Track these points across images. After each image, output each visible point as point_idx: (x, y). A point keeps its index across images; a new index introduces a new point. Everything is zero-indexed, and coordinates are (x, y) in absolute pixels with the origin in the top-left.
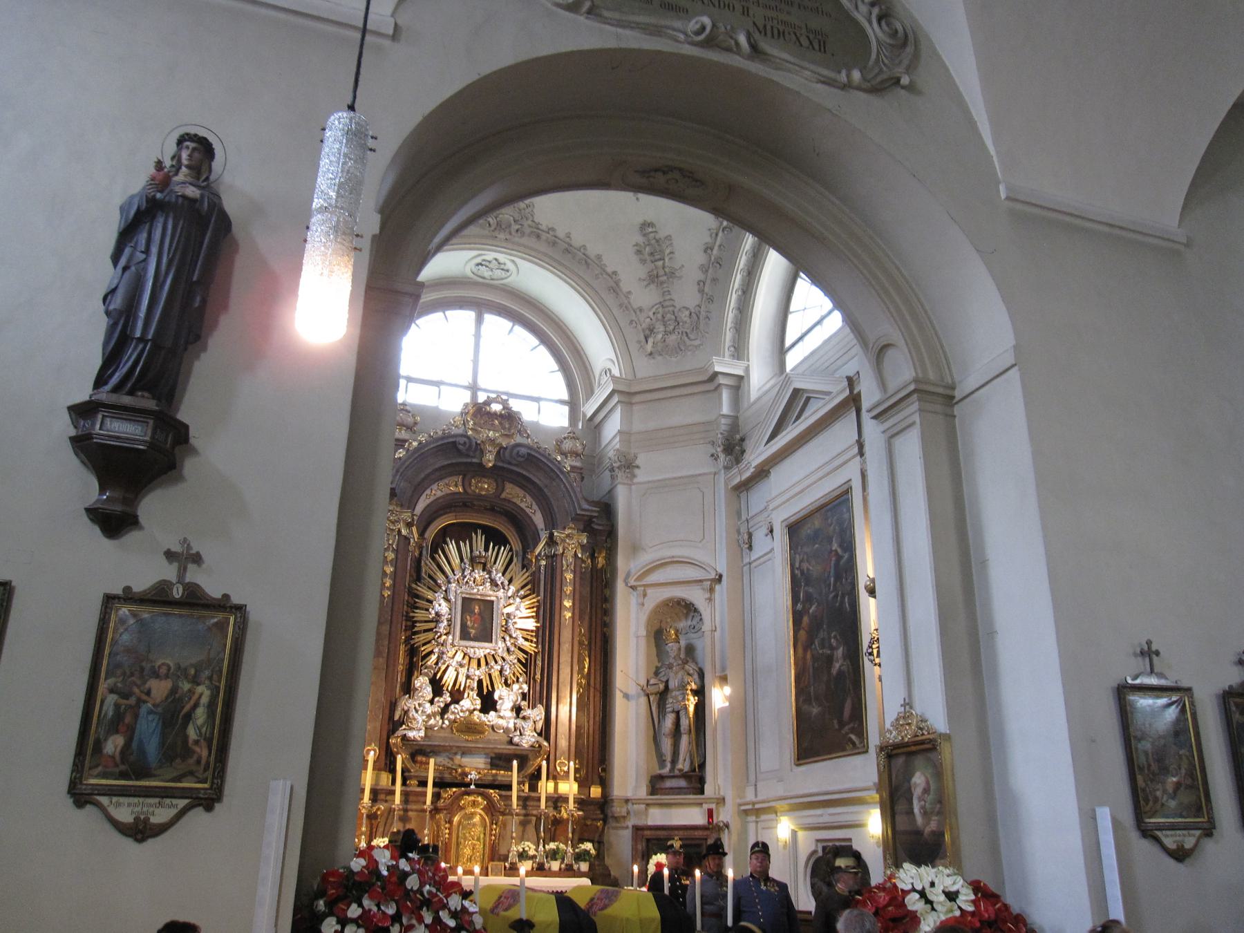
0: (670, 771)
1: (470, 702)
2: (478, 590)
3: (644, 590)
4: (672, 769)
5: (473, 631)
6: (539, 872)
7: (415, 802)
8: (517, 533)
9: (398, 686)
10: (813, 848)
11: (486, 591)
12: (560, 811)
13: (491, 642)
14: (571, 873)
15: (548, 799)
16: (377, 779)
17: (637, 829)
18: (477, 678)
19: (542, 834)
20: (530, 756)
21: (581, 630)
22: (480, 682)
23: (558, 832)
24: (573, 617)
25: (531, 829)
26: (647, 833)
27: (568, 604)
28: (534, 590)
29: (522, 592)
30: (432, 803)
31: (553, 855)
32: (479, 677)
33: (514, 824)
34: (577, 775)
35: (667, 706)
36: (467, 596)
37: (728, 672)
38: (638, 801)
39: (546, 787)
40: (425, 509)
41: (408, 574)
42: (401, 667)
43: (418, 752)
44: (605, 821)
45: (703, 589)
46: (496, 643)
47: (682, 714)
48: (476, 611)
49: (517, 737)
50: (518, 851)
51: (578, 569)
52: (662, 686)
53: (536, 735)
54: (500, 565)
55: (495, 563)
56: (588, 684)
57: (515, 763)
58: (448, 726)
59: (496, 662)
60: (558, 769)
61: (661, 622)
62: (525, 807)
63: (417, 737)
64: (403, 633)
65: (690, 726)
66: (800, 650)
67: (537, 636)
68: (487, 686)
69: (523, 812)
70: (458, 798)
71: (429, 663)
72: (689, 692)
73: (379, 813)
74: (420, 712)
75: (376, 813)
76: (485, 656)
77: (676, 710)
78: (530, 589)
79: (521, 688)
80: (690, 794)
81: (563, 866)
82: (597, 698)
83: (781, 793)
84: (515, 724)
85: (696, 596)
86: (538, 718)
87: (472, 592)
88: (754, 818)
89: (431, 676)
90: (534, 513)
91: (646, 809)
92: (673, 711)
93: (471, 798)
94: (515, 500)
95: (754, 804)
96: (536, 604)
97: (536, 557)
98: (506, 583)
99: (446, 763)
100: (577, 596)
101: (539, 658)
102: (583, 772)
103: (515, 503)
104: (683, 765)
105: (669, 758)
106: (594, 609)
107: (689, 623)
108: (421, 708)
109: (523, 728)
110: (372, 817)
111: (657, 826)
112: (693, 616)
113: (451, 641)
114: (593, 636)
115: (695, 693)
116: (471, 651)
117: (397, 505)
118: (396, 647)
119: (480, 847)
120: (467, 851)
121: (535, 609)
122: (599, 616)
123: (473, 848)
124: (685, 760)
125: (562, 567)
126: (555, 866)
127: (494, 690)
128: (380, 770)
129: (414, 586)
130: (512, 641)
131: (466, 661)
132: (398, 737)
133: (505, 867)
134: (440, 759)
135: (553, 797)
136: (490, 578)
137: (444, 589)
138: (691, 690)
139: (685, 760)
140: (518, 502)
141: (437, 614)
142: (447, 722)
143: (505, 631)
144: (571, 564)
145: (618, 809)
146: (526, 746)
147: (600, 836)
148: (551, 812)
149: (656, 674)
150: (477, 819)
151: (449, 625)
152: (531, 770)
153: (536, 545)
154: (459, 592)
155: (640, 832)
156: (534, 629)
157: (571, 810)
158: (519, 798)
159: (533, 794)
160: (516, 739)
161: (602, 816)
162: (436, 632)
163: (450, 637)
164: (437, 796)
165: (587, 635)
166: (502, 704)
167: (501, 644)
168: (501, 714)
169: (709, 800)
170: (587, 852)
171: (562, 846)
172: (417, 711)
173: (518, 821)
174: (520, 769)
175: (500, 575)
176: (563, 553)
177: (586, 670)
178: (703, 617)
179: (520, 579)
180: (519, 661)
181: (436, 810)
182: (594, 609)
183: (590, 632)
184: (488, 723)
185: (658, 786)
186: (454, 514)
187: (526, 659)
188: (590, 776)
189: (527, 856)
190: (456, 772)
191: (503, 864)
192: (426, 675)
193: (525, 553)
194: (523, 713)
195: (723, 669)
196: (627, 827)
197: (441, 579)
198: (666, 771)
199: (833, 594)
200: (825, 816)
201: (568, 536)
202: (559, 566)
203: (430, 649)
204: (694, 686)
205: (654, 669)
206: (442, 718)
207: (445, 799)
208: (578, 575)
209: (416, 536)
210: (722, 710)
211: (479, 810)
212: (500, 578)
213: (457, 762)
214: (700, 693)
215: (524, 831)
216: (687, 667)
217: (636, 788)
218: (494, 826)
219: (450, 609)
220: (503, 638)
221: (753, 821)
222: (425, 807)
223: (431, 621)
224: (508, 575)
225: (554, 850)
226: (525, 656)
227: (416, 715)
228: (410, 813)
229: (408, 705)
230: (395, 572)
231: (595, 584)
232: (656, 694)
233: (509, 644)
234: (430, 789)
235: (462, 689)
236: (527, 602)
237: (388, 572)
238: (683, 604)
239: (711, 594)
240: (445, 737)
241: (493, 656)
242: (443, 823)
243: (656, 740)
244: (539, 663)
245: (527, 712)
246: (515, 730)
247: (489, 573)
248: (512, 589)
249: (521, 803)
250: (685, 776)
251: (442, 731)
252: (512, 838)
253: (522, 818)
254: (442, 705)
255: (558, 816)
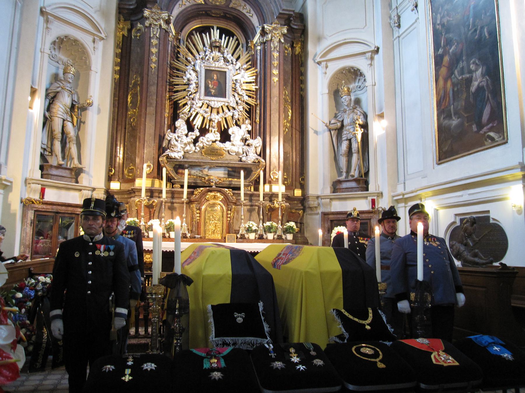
0: (345, 178)
1: (213, 136)
2: (215, 65)
3: (326, 64)
4: (347, 177)
5: (213, 91)
6: (260, 240)
7: (178, 198)
8: (243, 33)
9: (166, 126)
10: (453, 220)
11: (220, 65)
12: (274, 203)
13: (226, 97)
14: (281, 240)
15: (265, 195)
16: (153, 184)
17: (324, 214)
18: (216, 121)
19: (262, 217)
20: (253, 168)
21: (285, 93)
22: (219, 123)
23: (273, 216)
24: (279, 81)
25: (255, 214)
26: (331, 217)
27: (275, 72)
28: (254, 65)
29: (245, 66)
30: (187, 198)
31: (269, 229)
32: (218, 119)
33: (243, 210)
34: (286, 182)
35: (343, 136)
36: (208, 68)
37: (384, 111)
38: (325, 197)
39: (264, 189)
40: (179, 14)
41: (169, 56)
42: (166, 115)
43: (179, 166)
44: (304, 210)
45: (367, 58)
46: (229, 98)
47: (353, 141)
48: (215, 78)
49: (244, 157)
50: (245, 227)
51: (281, 51)
52: (339, 124)
53: (256, 155)
54: (230, 49)
55: (227, 47)
56: (292, 127)
57: (242, 173)
58: (199, 151)
59: (229, 110)
60: (272, 177)
61: (338, 85)
62: (251, 200)
63: (177, 157)
64: (167, 93)
65: (358, 148)
66: (441, 82)
67: (256, 95)
68: (224, 126)
69: (249, 203)
70: (204, 194)
71: (185, 111)
72: (357, 125)
73: (154, 204)
74: (179, 142)
75: (152, 204)
76: (222, 107)
77: (348, 138)
78: (250, 65)
79: (247, 127)
80: (359, 191)
81: (276, 236)
82: (298, 136)
83: (425, 183)
84: (243, 149)
85: (361, 64)
86: (258, 145)
87: (211, 66)
88: (403, 204)
89: (186, 119)
90: (252, 16)
91: (330, 202)
92: (347, 140)
93: (213, 194)
94: (238, 8)
95: (403, 195)
96: (255, 74)
97: (254, 45)
98: (234, 60)
99: (198, 174)
100: (282, 68)
101: (258, 108)
102: (289, 181)
103: (239, 10)
104: (355, 173)
105: (344, 170)
106: (294, 80)
107: (357, 84)
108: (180, 139)
109: (248, 151)
110: (149, 207)
111: (338, 212)
112: (359, 80)
113: (198, 97)
114: (294, 97)
115: (361, 126)
116: (212, 104)
117: (158, 8)
118: (162, 100)
119: (219, 224)
120: (212, 227)
121: (254, 77)
122: (298, 84)
123: (216, 226)
124: (355, 170)
125: (271, 49)
126: (270, 236)
127: (228, 128)
128: (154, 178)
129: (172, 62)
130: (240, 97)
131: (209, 110)
132: (165, 156)
133: (237, 238)
134: (193, 172)
135: (269, 194)
136: (223, 57)
137: (193, 63)
138: (359, 124)
139: (355, 170)
140: (241, 10)
141: (189, 80)
142: (197, 148)
143: (235, 91)
144: (277, 47)
145: (312, 203)
146: (250, 162)
147: (301, 219)
148: (268, 204)
149: (336, 117)
150: (218, 208)
151: (197, 87)
152: (253, 177)
153: (254, 36)
154: (202, 65)
155: (326, 216)
156: (255, 90)
157: (280, 202)
158: (245, 194)
159: (255, 193)
160: (244, 159)
161: (302, 207)
162: (189, 91)
163: (198, 94)
164: (190, 194)
165: (290, 96)
166: (234, 137)
167: (232, 99)
168: (233, 143)
169: (372, 194)
170: (291, 228)
171: (275, 224)
172: (177, 141)
173: (246, 210)
174: (246, 178)
175: (230, 55)
176: (271, 39)
177: (290, 117)
178: (366, 78)
179: (244, 58)
180: (246, 111)
181: (190, 202)
182: (294, 80)
183: (292, 94)
184: (225, 149)
185: (338, 187)
186: (200, 20)
187: (249, 109)
188: (294, 183)
189: (251, 230)
190: (205, 179)
191: (235, 235)
192: (182, 118)
193: (247, 43)
194: (248, 142)
195: (381, 109)
196: (318, 214)
197: (190, 58)
198: (343, 178)
199: (473, 30)
200: (465, 196)
201: (274, 29)
202: (269, 48)
203: (185, 102)
204: (361, 122)
205: (334, 115)
206: (195, 146)
207: (196, 195)
208: (282, 54)
209: (174, 32)
210: (379, 137)
211: (218, 202)
212: (230, 58)
213: (205, 173)
214: (365, 126)
215: (251, 215)
216: (355, 110)
217: (323, 189)
218: (229, 212)
219: (197, 77)
220: (233, 95)
221: (402, 207)
222: (183, 200)
223: (185, 85)
224: (236, 56)
225: (269, 226)
226: (249, 107)
227: (176, 143)
228: (175, 205)
229: (170, 136)
230: (159, 52)
231: (294, 64)
232: (335, 130)
233: (237, 99)
234: (186, 190)
235: (207, 127)
236: (249, 73)
237: (154, 52)
238: (353, 70)
239: (371, 61)
240: (197, 158)
241: (227, 106)
242: (195, 209)
243: (336, 159)
244: (258, 111)
245: (250, 141)
246: (243, 153)
247: (223, 53)
248: (239, 64)
249: (248, 198)
250: (356, 180)
251: (195, 154)
252: (242, 219)
253: (249, 207)
254: (194, 137)
255: (272, 206)
